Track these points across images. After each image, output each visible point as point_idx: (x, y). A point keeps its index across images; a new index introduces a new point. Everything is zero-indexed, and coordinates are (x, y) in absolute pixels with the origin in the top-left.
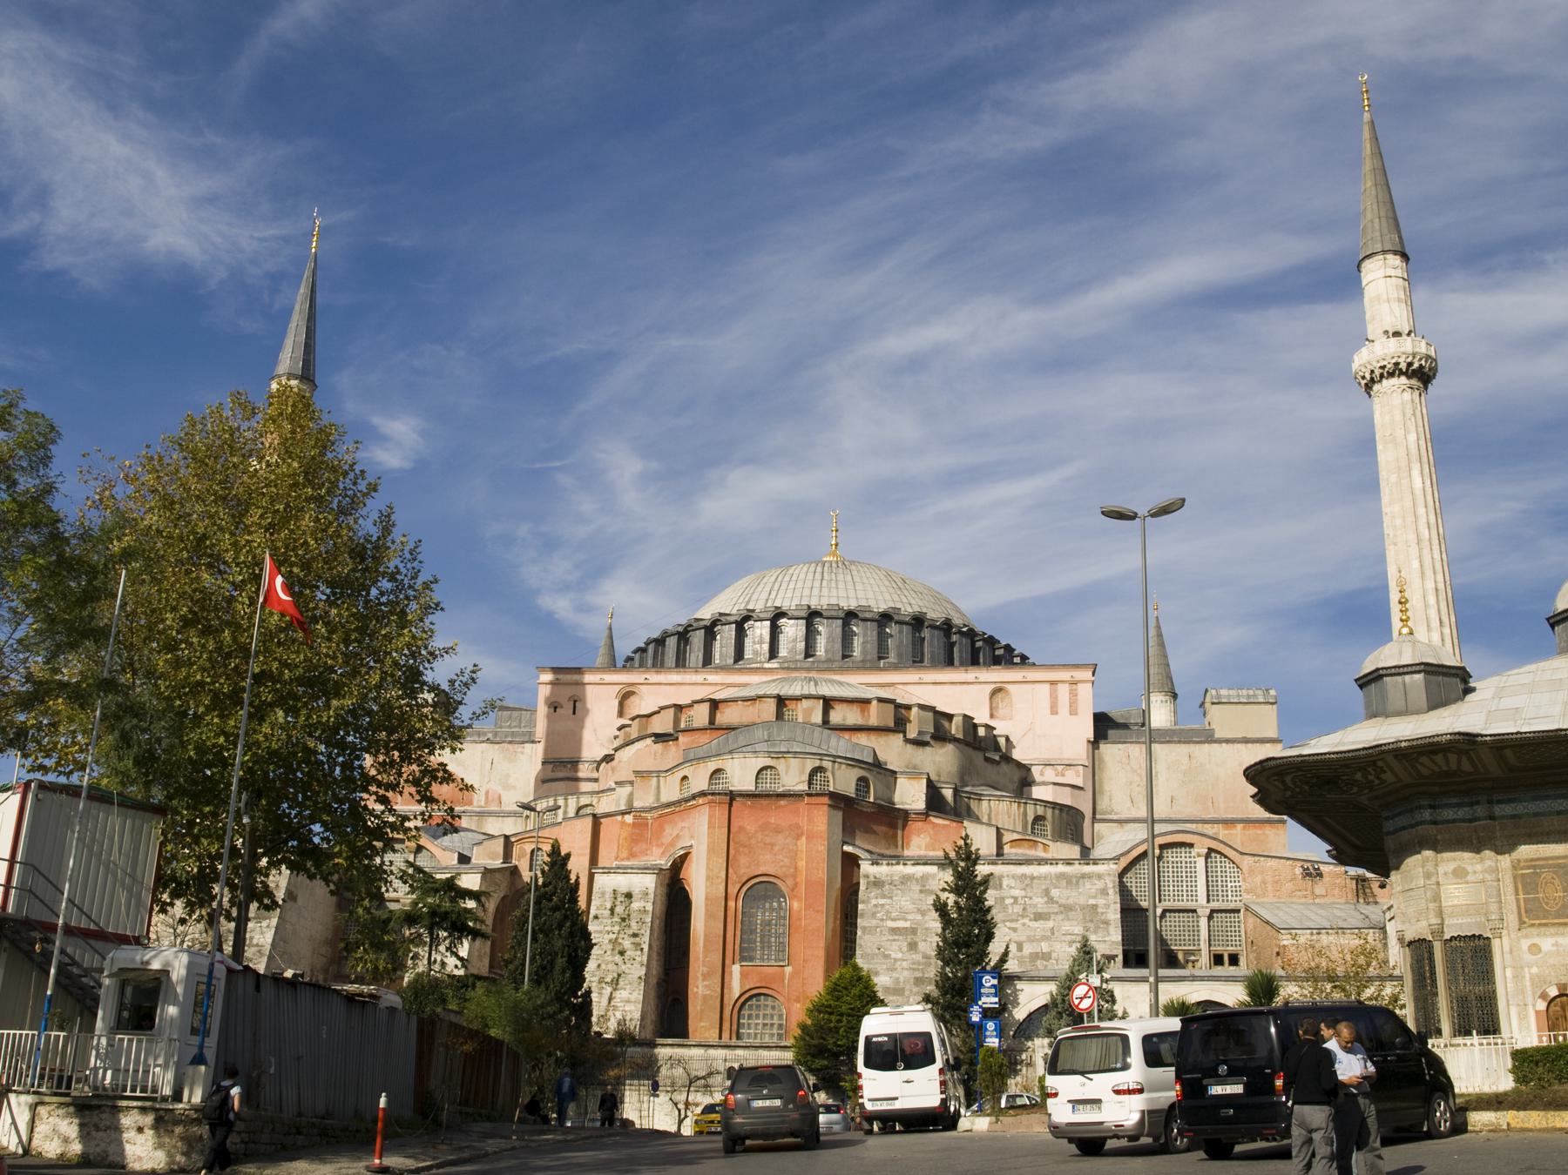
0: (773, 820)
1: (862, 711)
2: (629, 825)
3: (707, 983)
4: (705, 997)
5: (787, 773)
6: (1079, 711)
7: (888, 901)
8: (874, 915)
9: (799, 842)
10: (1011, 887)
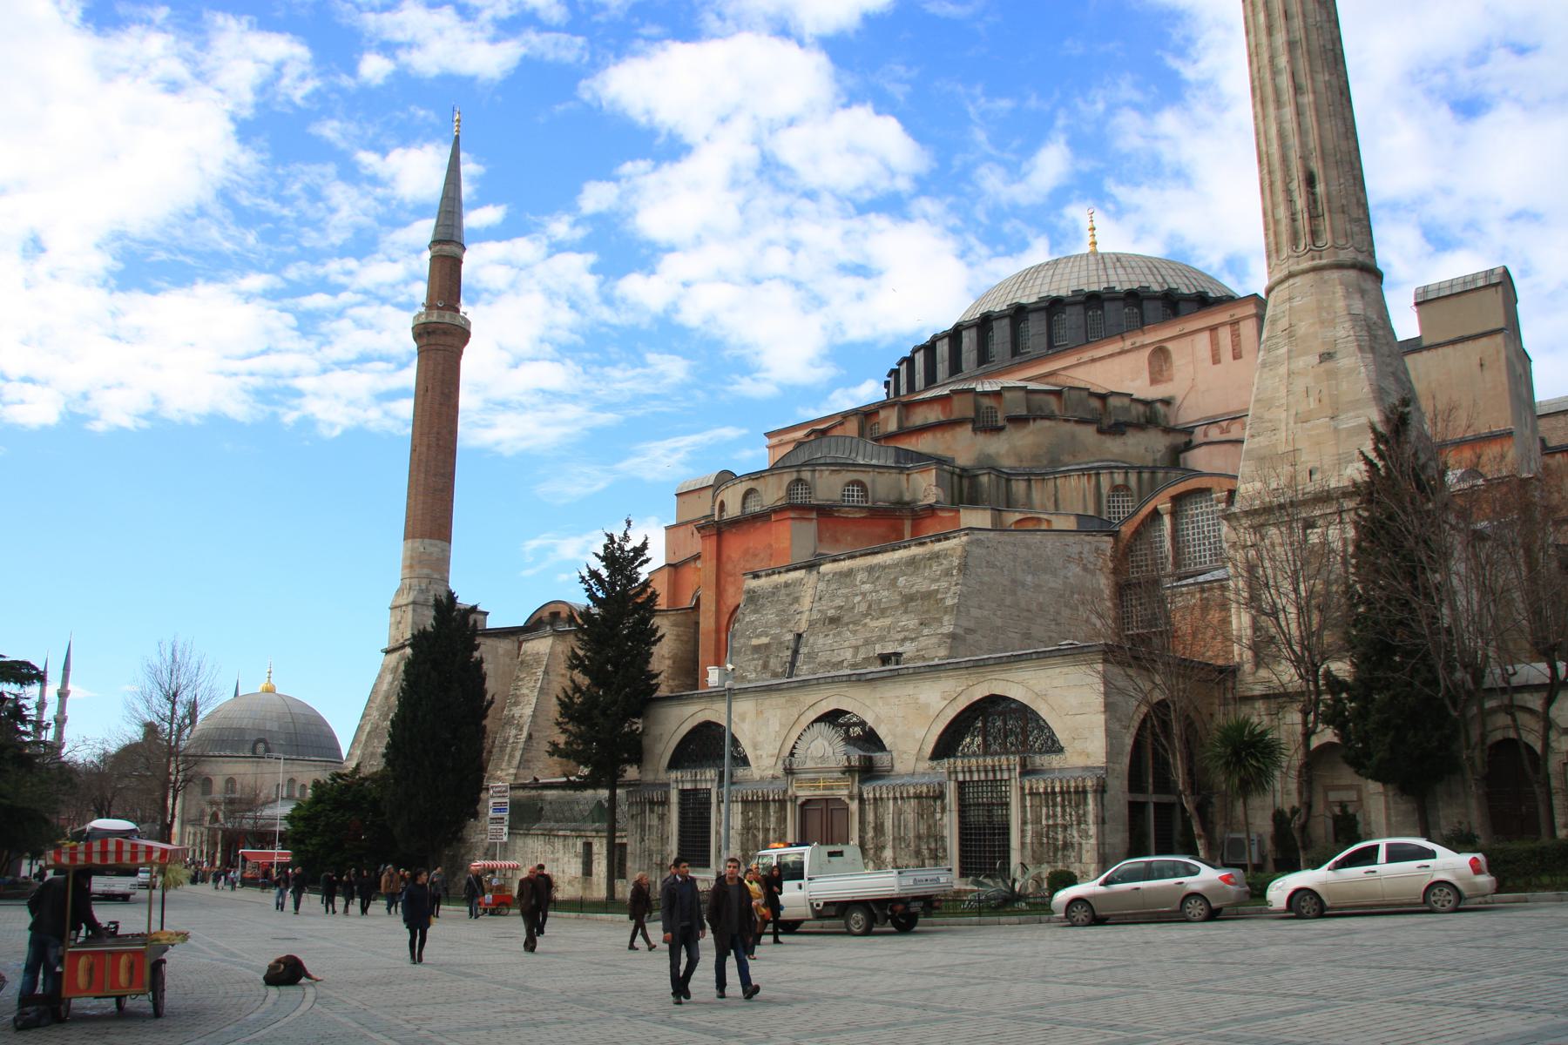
1: (944, 410)
6: (1243, 353)
10: (863, 583)
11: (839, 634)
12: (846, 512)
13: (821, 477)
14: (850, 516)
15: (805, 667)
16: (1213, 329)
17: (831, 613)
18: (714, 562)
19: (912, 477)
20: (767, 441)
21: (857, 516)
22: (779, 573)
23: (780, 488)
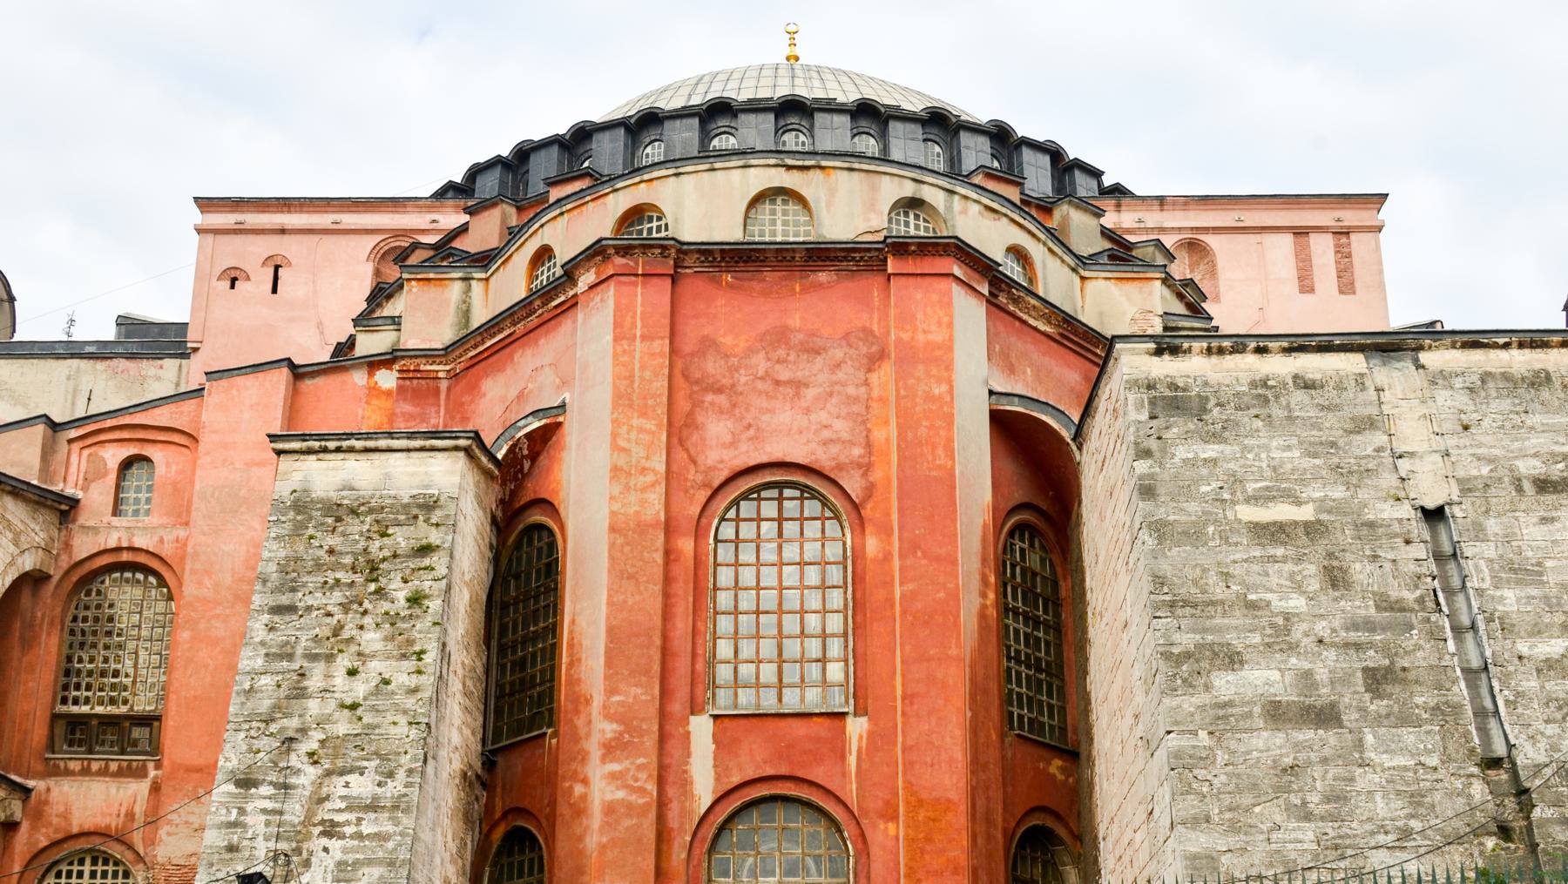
0: (795, 321)
2: (388, 393)
3: (615, 767)
4: (610, 809)
5: (829, 205)
6: (1358, 285)
7: (1228, 449)
9: (874, 378)
12: (1028, 313)
13: (964, 212)
14: (1032, 322)
15: (1510, 595)
16: (1300, 232)
17: (1529, 467)
18: (662, 346)
19: (1090, 285)
20: (196, 217)
21: (1043, 327)
22: (1261, 351)
23: (871, 206)
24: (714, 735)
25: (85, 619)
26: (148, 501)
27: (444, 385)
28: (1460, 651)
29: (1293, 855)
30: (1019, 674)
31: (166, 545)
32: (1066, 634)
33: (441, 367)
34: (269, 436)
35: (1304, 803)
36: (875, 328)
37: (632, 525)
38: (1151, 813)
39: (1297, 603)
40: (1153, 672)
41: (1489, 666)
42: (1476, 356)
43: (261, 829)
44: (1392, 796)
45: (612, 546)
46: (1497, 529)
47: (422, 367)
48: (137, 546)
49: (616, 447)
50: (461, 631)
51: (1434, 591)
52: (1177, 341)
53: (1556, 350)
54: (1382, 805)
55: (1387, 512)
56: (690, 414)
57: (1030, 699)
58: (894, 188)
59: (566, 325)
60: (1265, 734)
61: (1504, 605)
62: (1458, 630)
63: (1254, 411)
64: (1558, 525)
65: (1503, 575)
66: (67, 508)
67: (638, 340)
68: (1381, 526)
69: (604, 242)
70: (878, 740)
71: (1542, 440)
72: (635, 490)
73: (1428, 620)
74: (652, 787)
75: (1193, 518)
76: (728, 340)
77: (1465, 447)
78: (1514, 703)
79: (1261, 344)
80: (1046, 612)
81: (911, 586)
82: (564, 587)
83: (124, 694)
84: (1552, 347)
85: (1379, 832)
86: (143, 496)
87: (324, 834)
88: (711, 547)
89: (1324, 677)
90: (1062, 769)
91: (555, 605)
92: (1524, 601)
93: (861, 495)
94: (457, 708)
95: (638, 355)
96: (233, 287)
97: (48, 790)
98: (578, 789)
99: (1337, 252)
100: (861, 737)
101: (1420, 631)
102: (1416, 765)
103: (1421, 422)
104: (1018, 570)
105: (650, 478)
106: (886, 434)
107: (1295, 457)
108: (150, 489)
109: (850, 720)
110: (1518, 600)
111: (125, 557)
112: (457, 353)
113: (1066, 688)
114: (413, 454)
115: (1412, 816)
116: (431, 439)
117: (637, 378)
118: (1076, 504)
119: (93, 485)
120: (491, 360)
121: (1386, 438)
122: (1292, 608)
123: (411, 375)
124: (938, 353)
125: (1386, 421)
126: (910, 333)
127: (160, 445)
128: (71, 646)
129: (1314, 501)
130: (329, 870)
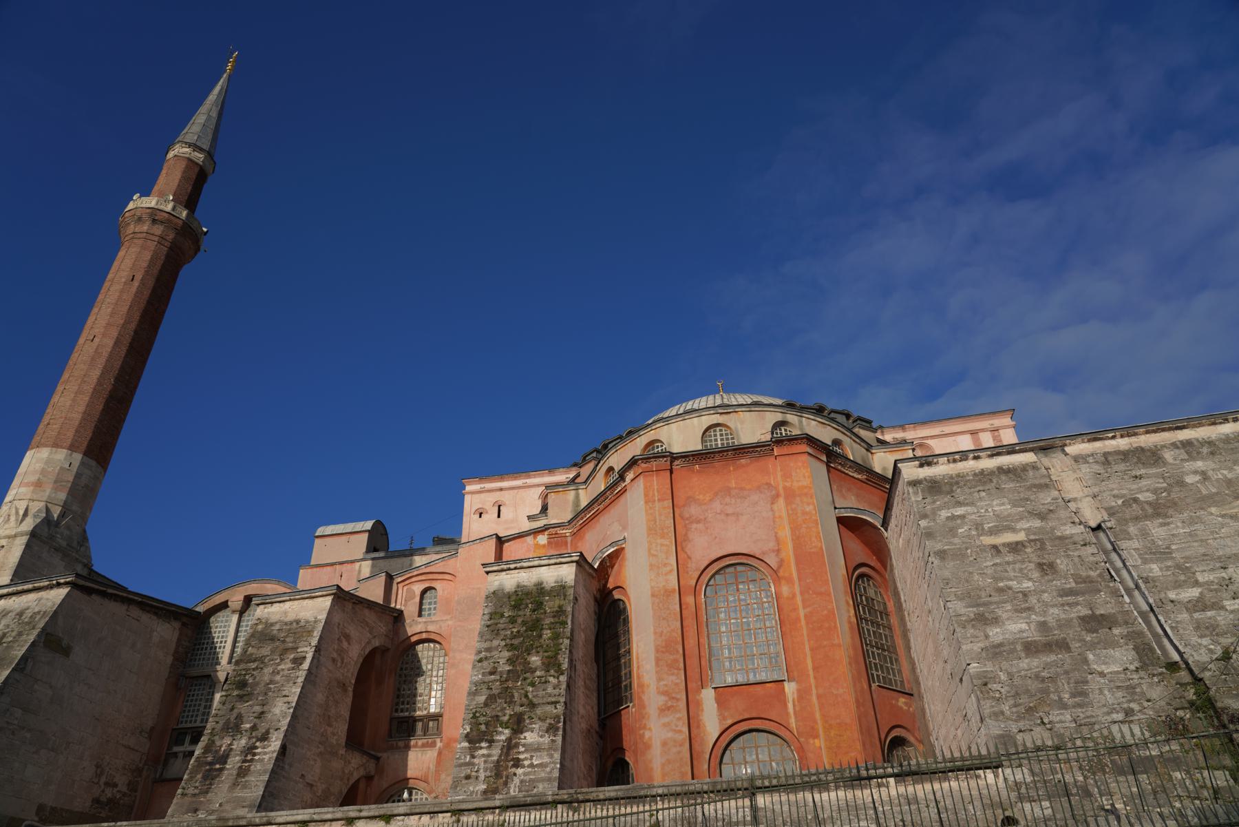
2: (544, 546)
3: (666, 720)
7: (969, 509)
8: (952, 532)
9: (775, 507)
11: (1200, 520)
13: (808, 424)
15: (1154, 566)
21: (856, 475)
22: (976, 458)
24: (715, 699)
25: (406, 669)
26: (435, 609)
27: (569, 539)
28: (1133, 601)
29: (1062, 731)
30: (873, 653)
31: (443, 629)
32: (895, 629)
33: (567, 531)
34: (482, 565)
35: (1060, 699)
36: (772, 482)
37: (662, 592)
38: (965, 716)
39: (1027, 585)
40: (952, 632)
41: (1154, 608)
42: (1098, 444)
43: (482, 765)
44: (1114, 690)
45: (653, 604)
46: (1136, 532)
47: (558, 532)
48: (429, 630)
49: (650, 555)
50: (581, 654)
51: (1108, 570)
52: (930, 459)
53: (1143, 436)
54: (1109, 696)
55: (1069, 530)
56: (686, 535)
57: (881, 666)
58: (774, 417)
59: (622, 499)
60: (1027, 661)
61: (1153, 573)
62: (1129, 592)
63: (978, 488)
64: (1172, 526)
65: (1147, 556)
66: (397, 615)
67: (657, 502)
68: (1067, 538)
69: (636, 458)
70: (803, 695)
71: (1149, 482)
72: (662, 574)
73: (1109, 587)
74: (686, 730)
75: (958, 546)
76: (701, 497)
77: (1104, 491)
78: (1176, 627)
79: (976, 455)
80: (882, 619)
81: (808, 610)
82: (632, 630)
83: (425, 705)
84: (1140, 434)
85: (1112, 712)
86: (432, 606)
87: (513, 766)
88: (703, 600)
89: (1054, 624)
90: (906, 704)
91: (629, 639)
92: (1164, 569)
93: (776, 566)
94: (581, 694)
95: (657, 509)
96: (480, 517)
97: (388, 757)
98: (647, 734)
99: (994, 440)
100: (793, 693)
101: (1106, 593)
102: (1124, 670)
103: (1075, 482)
104: (864, 598)
105: (668, 568)
106: (786, 533)
107: (1006, 508)
108: (435, 603)
109: (786, 684)
110: (1161, 569)
111: (424, 636)
112: (574, 523)
113: (900, 659)
114: (551, 567)
115: (1130, 701)
116: (557, 559)
117: (658, 521)
118: (889, 560)
119: (409, 603)
120: (590, 523)
121: (1057, 492)
122: (1025, 588)
123: (554, 536)
124: (806, 491)
125: (1055, 483)
126: (790, 483)
127: (439, 581)
128: (399, 683)
129: (1024, 530)
130: (517, 786)
